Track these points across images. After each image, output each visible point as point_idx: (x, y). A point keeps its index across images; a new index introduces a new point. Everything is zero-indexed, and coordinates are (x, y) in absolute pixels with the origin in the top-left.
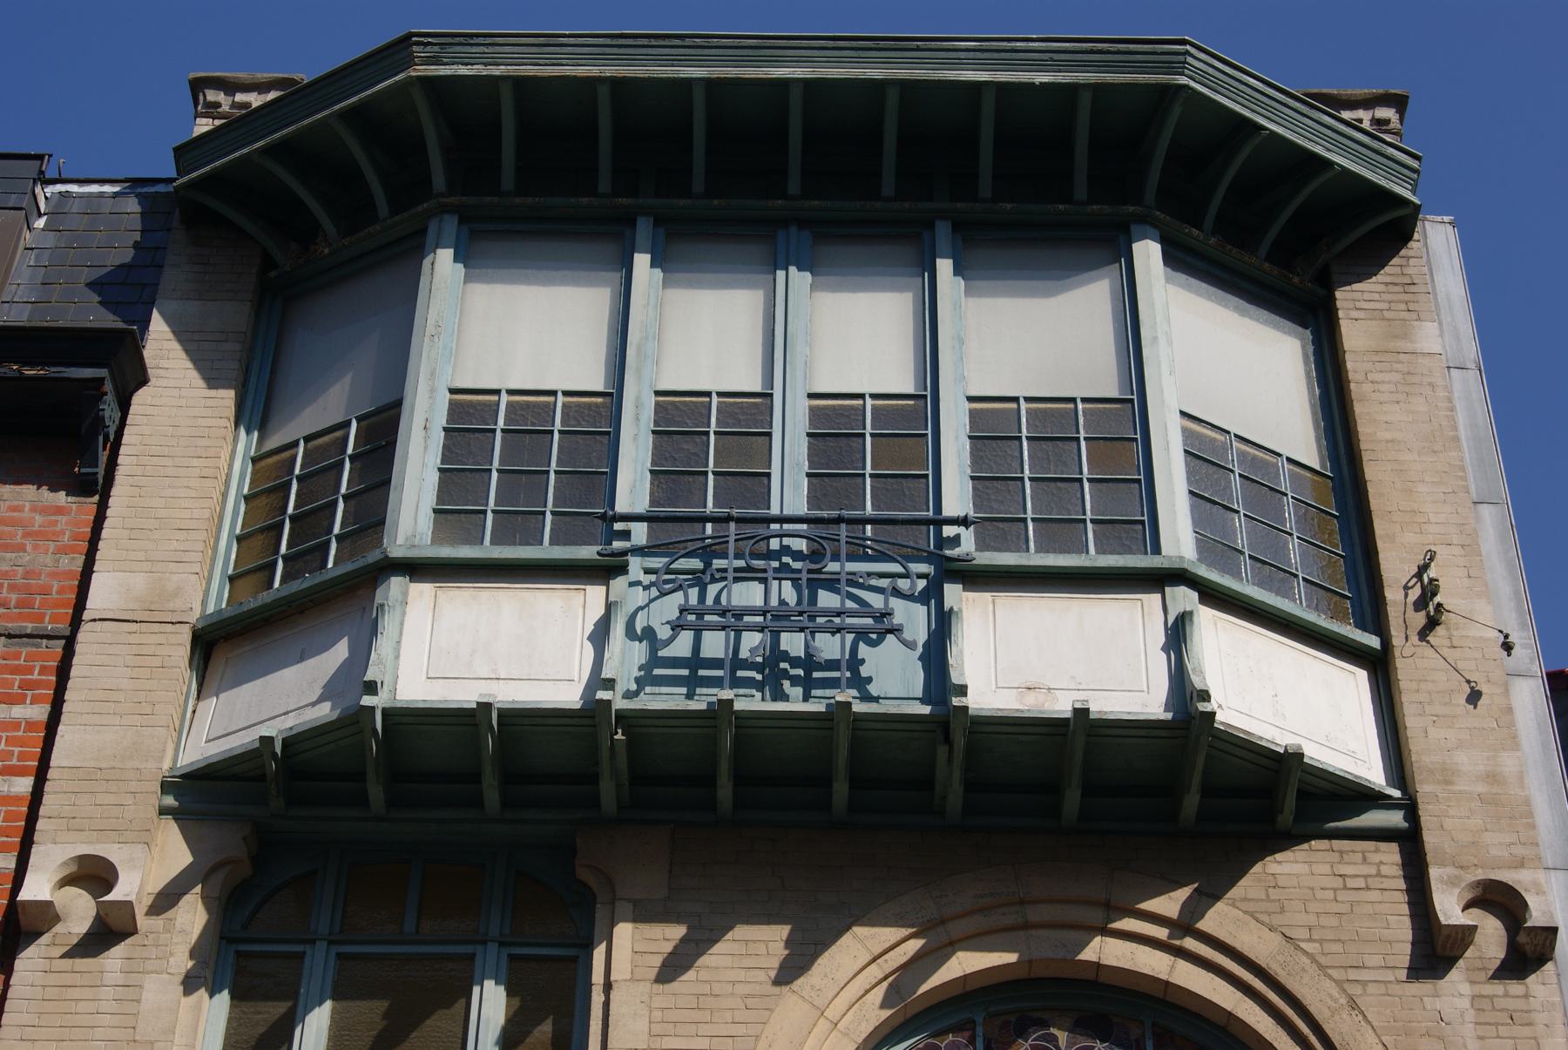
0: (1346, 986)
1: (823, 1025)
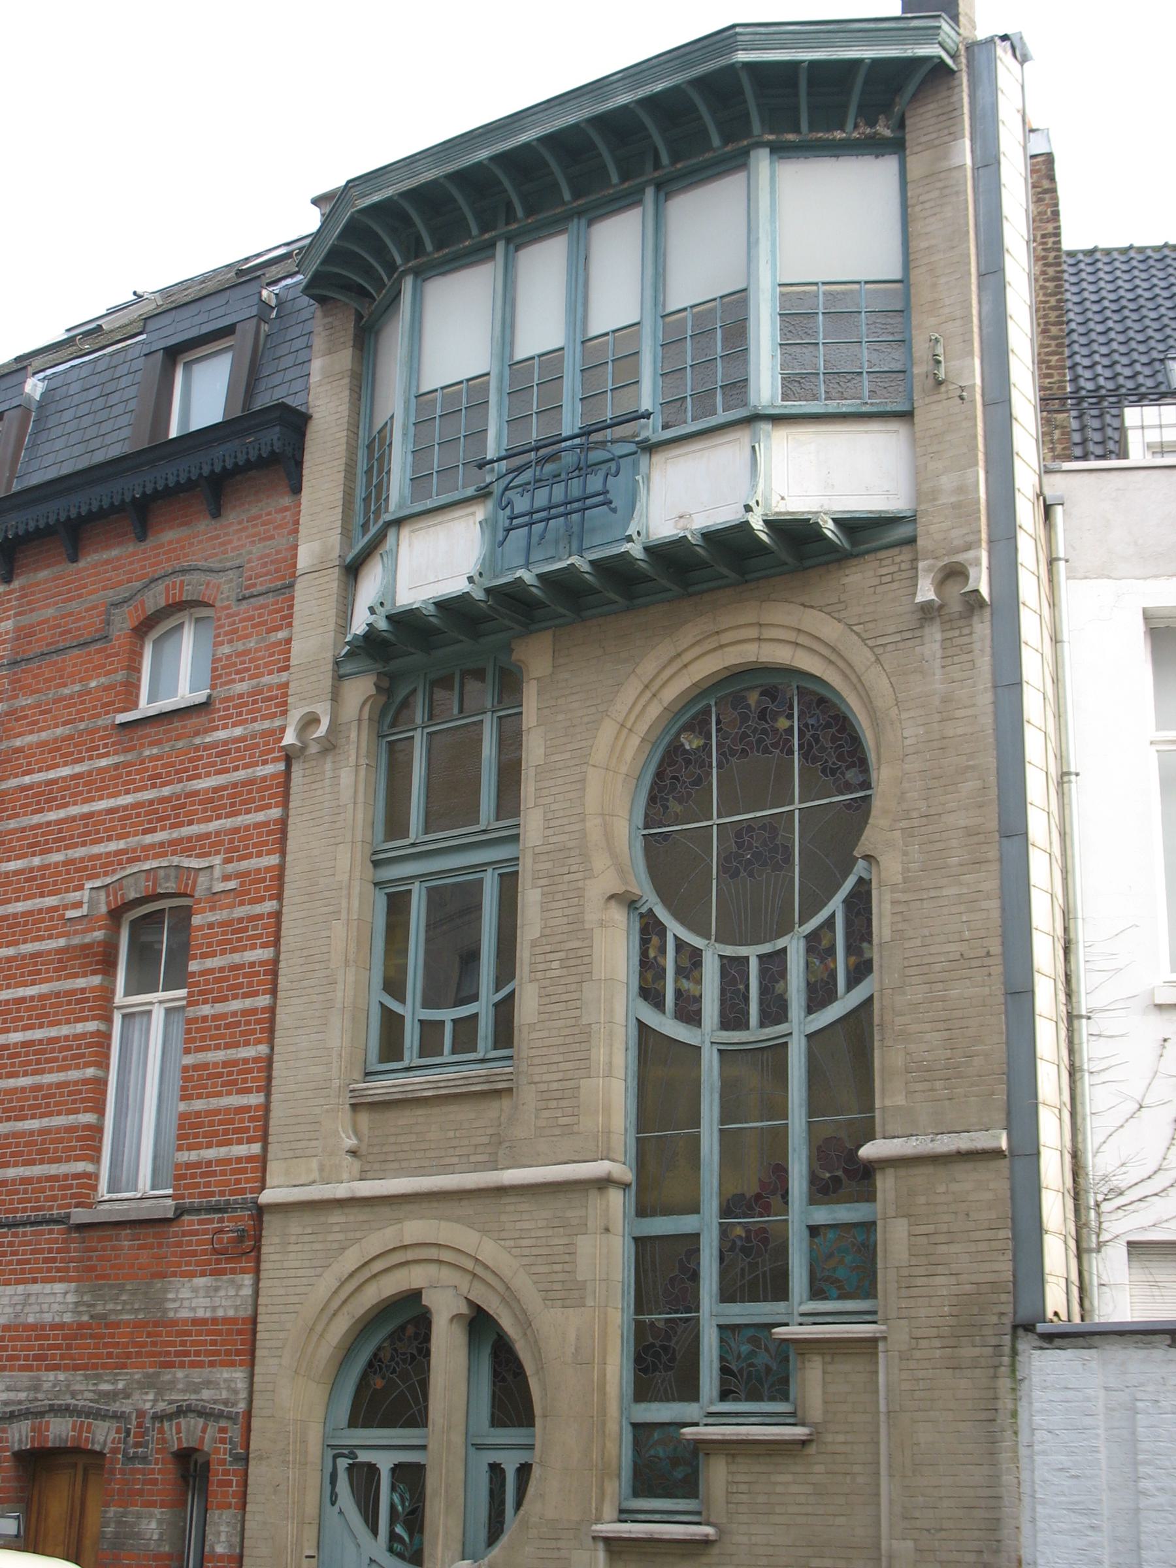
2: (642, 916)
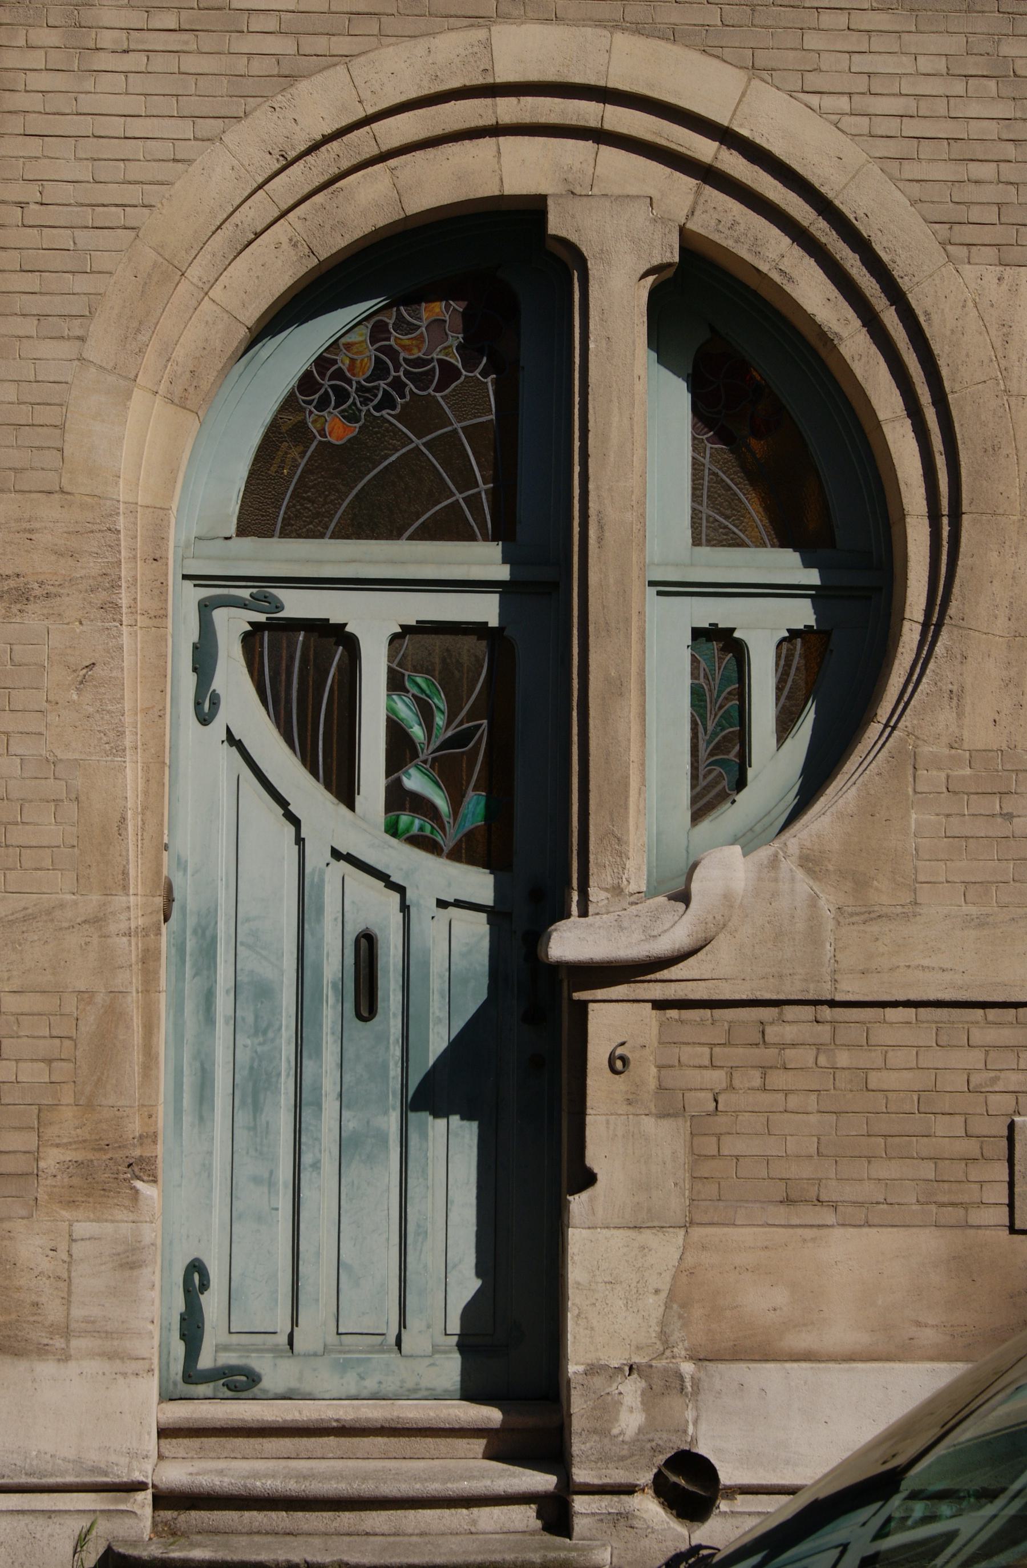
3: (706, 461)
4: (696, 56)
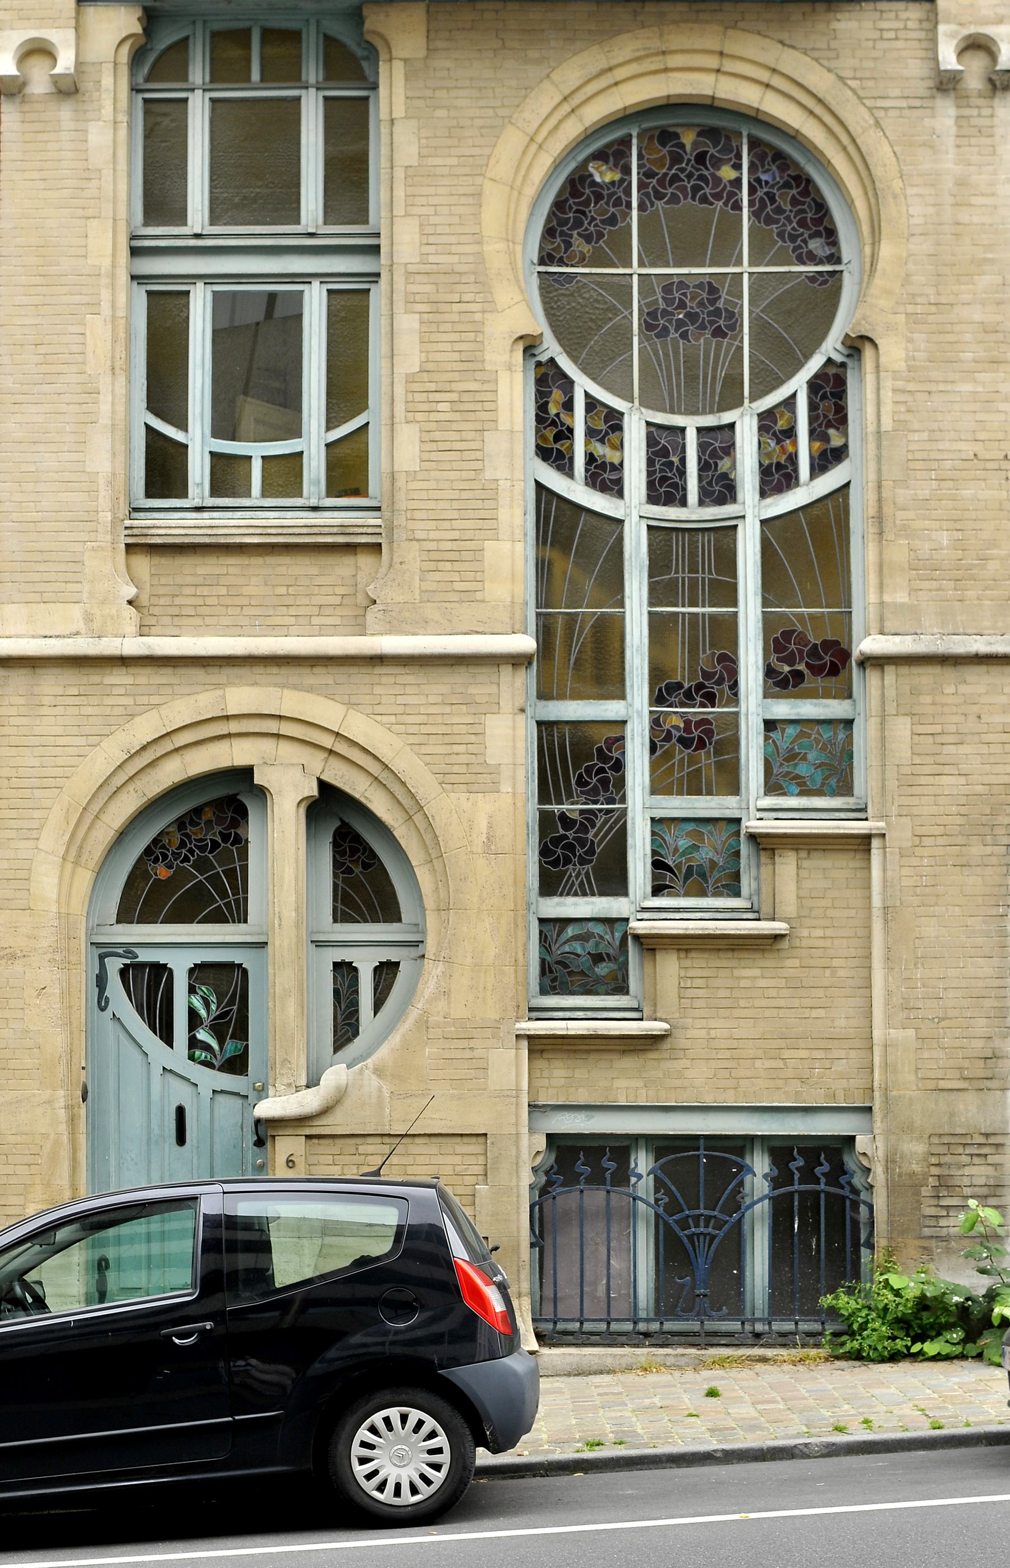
0: (874, 111)
1: (534, 147)
2: (539, 364)
3: (340, 883)
4: (321, 699)
